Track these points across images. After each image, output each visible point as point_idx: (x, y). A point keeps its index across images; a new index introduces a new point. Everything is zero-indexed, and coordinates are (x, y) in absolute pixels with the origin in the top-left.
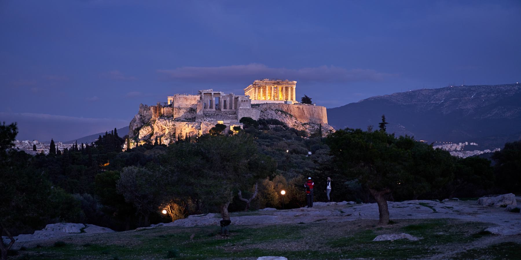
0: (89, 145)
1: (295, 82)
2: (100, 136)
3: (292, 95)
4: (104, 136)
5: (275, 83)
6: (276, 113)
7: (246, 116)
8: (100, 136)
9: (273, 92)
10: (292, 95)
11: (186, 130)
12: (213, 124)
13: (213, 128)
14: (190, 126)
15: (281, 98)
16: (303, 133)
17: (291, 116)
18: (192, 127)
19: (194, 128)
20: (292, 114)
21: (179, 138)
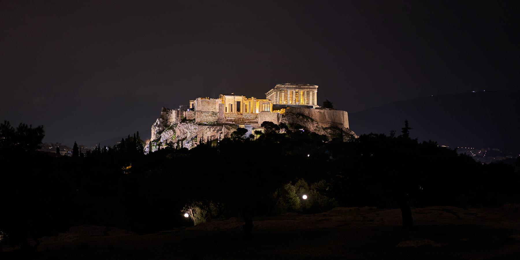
0: (112, 147)
1: (317, 87)
2: (123, 139)
3: (313, 100)
4: (126, 139)
5: (296, 88)
6: (298, 118)
7: (267, 121)
8: (123, 139)
9: (294, 96)
10: (313, 100)
11: (208, 134)
12: (235, 128)
13: (234, 132)
14: (212, 130)
15: (302, 102)
16: (324, 137)
17: (312, 120)
18: (214, 131)
19: (216, 131)
20: (313, 118)
21: (200, 142)
